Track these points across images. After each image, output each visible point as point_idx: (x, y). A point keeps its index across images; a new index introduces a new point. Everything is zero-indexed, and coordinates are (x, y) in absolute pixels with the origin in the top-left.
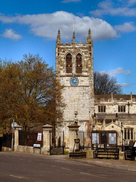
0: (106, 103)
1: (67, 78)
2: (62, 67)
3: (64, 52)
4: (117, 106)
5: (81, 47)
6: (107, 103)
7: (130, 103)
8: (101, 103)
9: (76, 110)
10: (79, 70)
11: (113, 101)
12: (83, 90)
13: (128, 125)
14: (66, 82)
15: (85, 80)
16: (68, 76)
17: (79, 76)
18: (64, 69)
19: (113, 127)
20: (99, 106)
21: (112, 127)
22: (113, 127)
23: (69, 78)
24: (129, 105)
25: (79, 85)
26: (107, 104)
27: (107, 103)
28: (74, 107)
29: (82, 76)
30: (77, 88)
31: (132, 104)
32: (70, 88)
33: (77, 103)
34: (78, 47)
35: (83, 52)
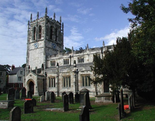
0: (55, 58)
1: (33, 43)
2: (31, 37)
3: (32, 27)
4: (62, 60)
5: (41, 20)
6: (56, 58)
7: (71, 56)
8: (52, 58)
9: (36, 66)
10: (40, 36)
11: (60, 56)
12: (40, 50)
13: (51, 74)
14: (32, 47)
15: (42, 43)
16: (33, 42)
17: (39, 41)
18: (32, 38)
19: (31, 75)
20: (51, 61)
21: (31, 75)
22: (31, 75)
23: (34, 43)
24: (71, 57)
25: (38, 48)
26: (56, 59)
27: (56, 58)
28: (35, 64)
29: (40, 41)
30: (38, 49)
31: (73, 57)
32: (34, 50)
33: (37, 61)
34: (39, 21)
35: (42, 24)
